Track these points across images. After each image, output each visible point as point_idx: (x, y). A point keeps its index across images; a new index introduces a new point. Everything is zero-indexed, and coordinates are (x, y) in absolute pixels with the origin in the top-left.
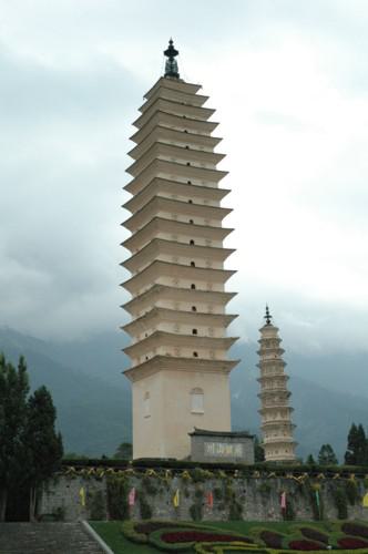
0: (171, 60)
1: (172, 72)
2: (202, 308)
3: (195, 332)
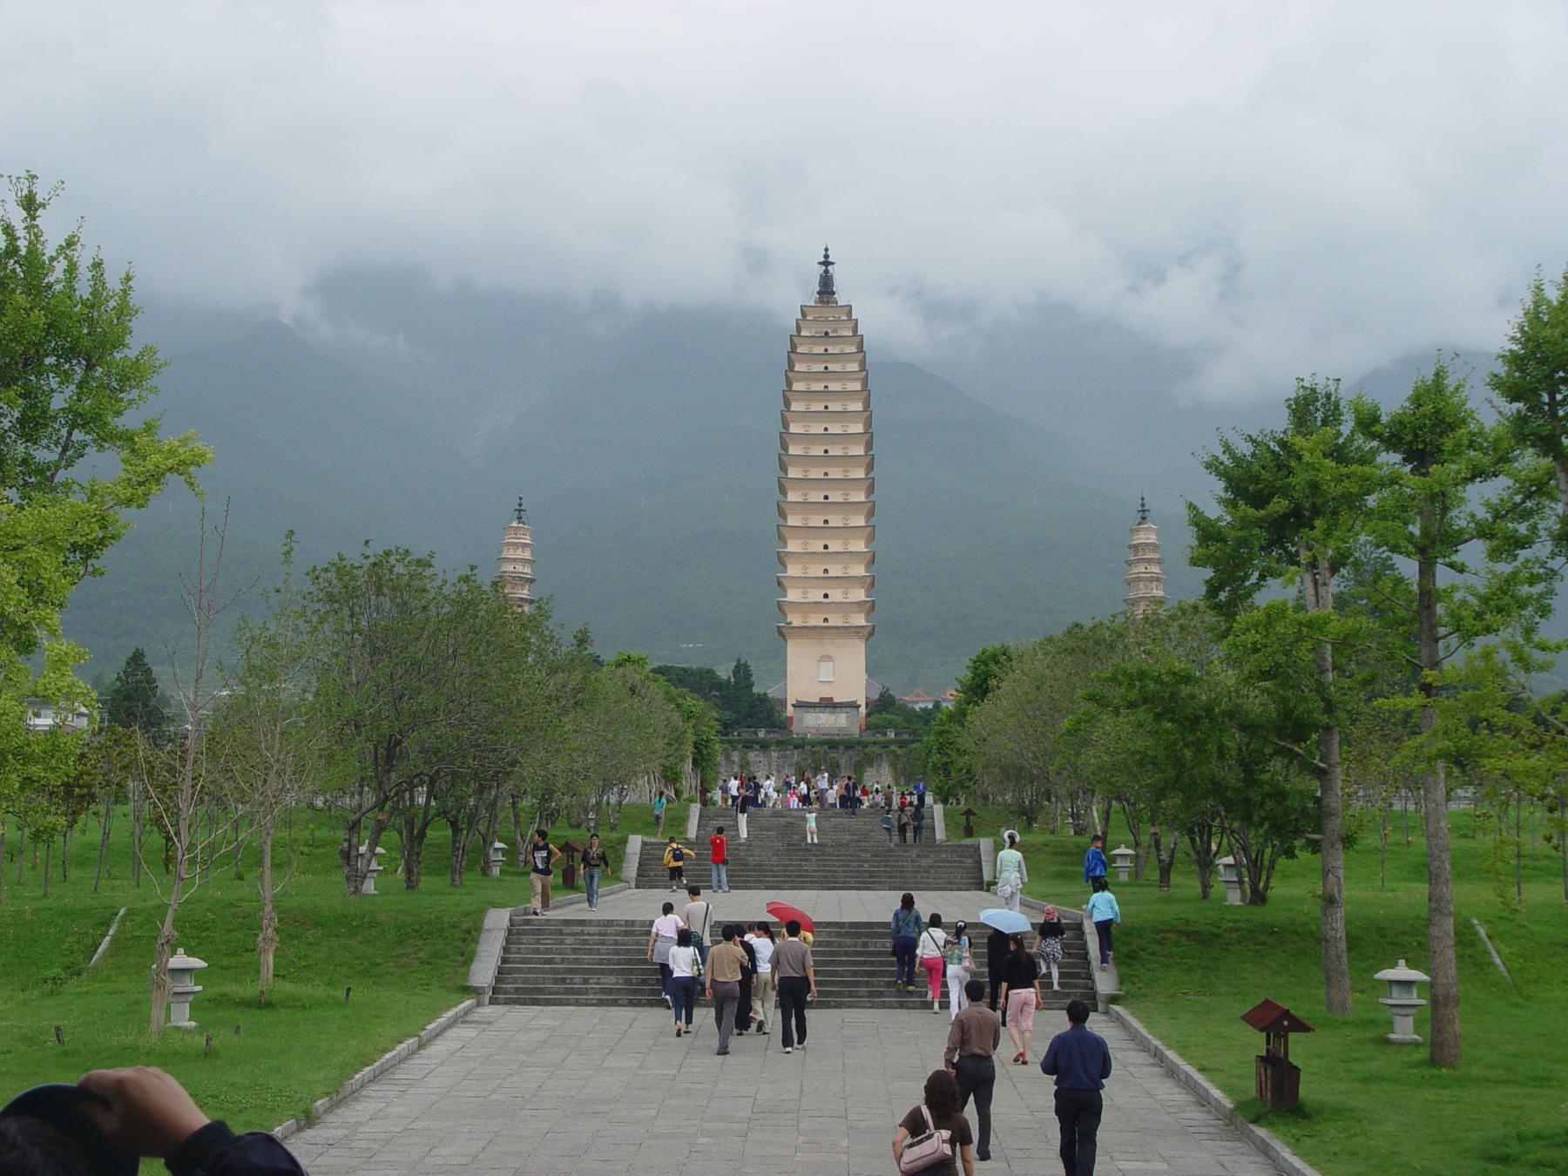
0: (826, 271)
1: (826, 288)
2: (836, 571)
3: (826, 596)
